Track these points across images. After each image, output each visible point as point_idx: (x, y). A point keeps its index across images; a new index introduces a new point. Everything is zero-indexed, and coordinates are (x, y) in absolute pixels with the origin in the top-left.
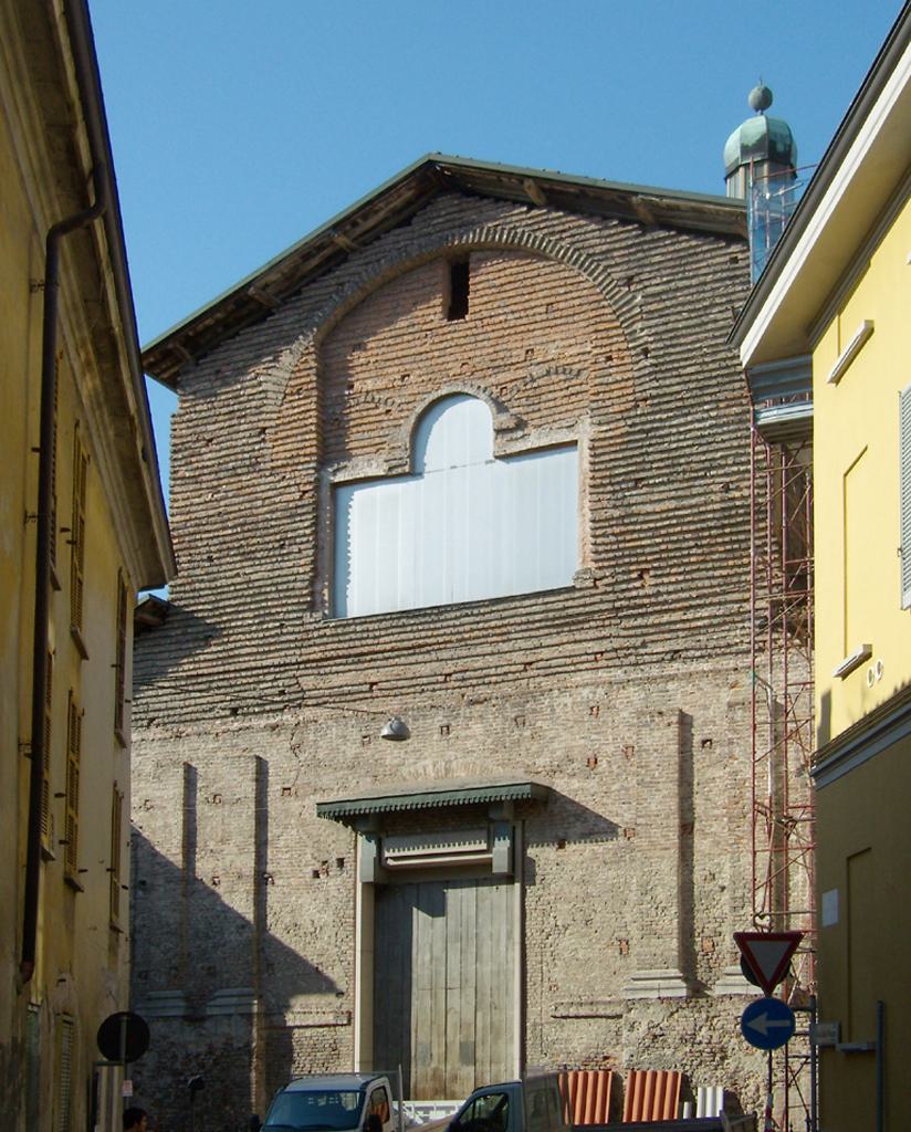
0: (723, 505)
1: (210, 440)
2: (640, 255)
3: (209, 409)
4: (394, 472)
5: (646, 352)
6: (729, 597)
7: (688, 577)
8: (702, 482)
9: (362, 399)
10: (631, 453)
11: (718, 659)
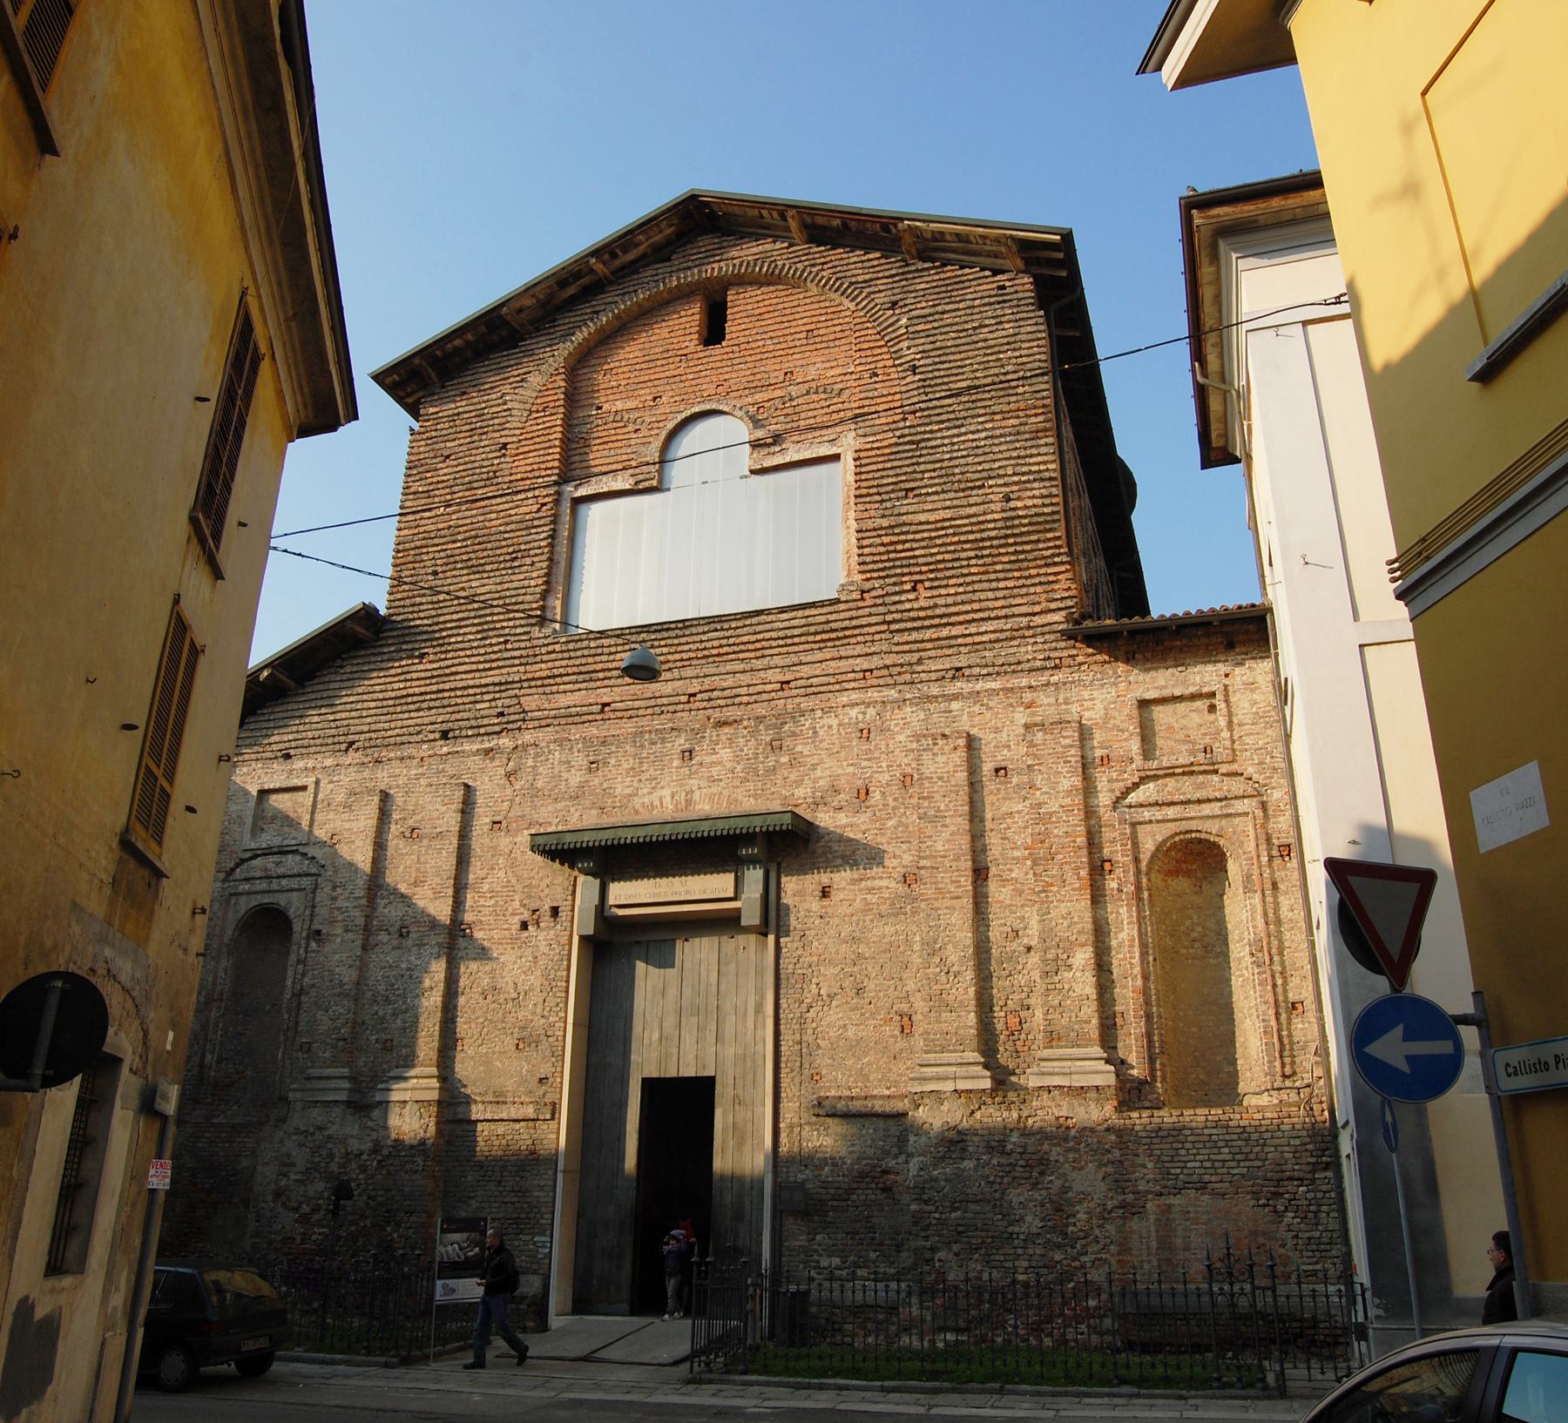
0: (1004, 515)
1: (448, 457)
2: (904, 283)
3: (451, 427)
4: (640, 487)
5: (914, 368)
6: (1016, 610)
7: (970, 588)
8: (980, 492)
9: (611, 419)
10: (900, 463)
11: (1008, 676)
